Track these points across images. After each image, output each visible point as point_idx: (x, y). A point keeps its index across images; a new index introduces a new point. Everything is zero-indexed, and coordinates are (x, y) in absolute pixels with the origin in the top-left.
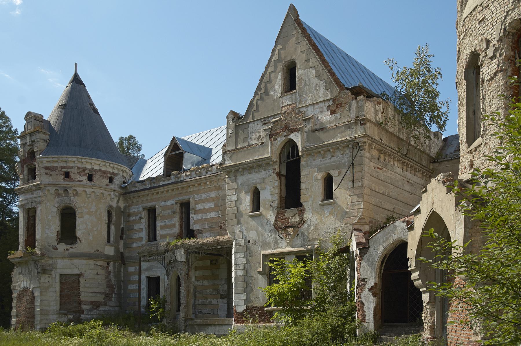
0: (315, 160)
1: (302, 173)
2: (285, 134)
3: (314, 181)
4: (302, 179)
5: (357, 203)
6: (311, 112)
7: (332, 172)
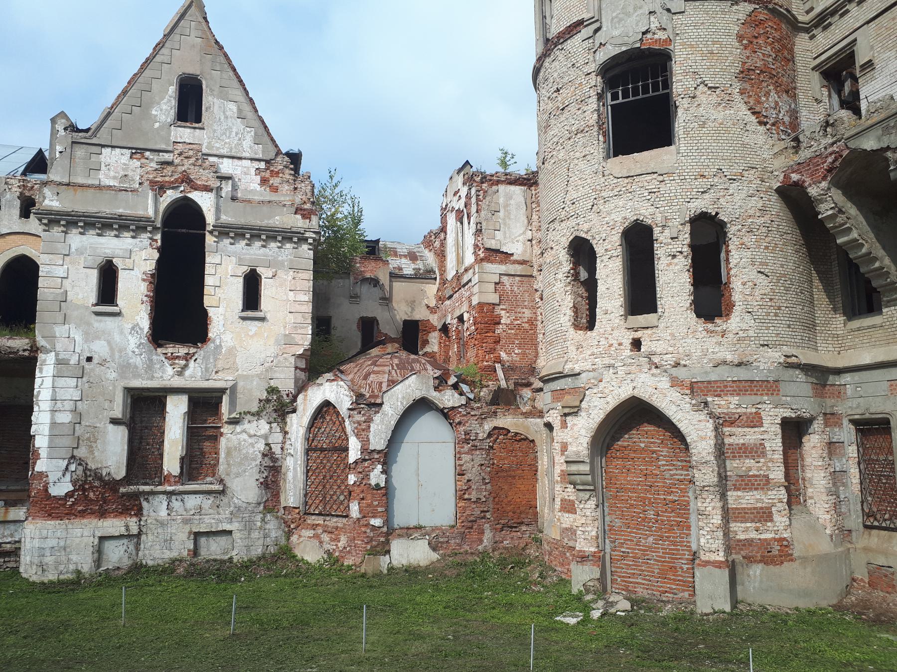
0: (231, 244)
1: (209, 259)
2: (182, 188)
3: (229, 277)
4: (209, 269)
5: (301, 325)
6: (226, 166)
7: (259, 270)
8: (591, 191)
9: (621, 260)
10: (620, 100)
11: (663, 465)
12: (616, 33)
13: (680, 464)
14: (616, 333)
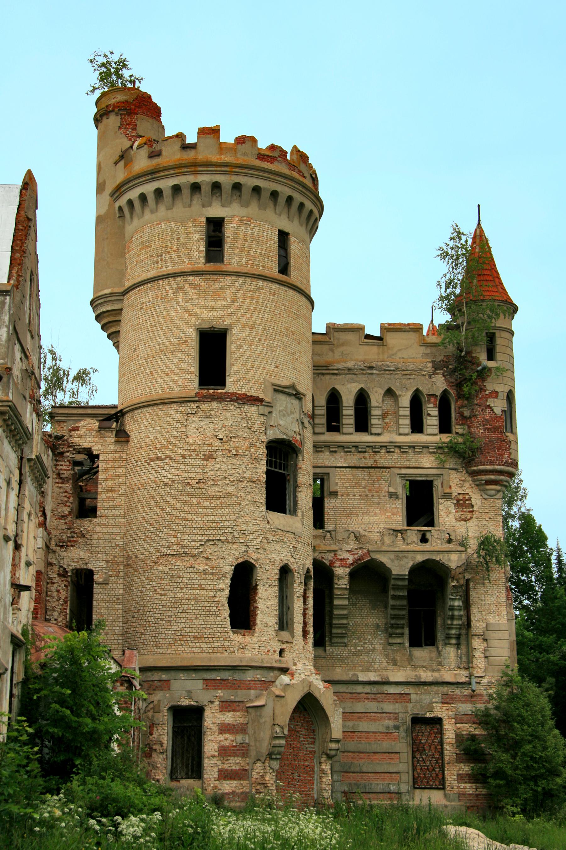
8: (260, 531)
9: (277, 589)
10: (273, 469)
11: (302, 741)
12: (282, 423)
13: (310, 740)
14: (272, 643)
